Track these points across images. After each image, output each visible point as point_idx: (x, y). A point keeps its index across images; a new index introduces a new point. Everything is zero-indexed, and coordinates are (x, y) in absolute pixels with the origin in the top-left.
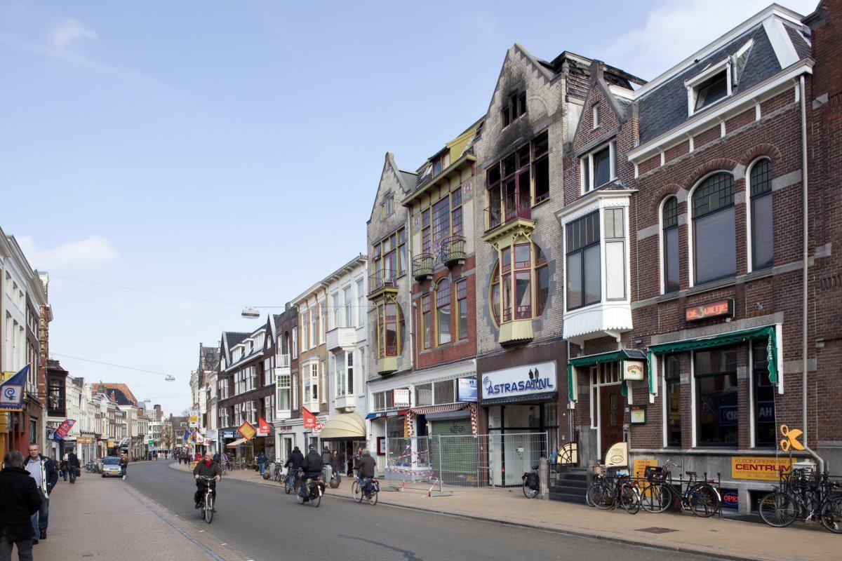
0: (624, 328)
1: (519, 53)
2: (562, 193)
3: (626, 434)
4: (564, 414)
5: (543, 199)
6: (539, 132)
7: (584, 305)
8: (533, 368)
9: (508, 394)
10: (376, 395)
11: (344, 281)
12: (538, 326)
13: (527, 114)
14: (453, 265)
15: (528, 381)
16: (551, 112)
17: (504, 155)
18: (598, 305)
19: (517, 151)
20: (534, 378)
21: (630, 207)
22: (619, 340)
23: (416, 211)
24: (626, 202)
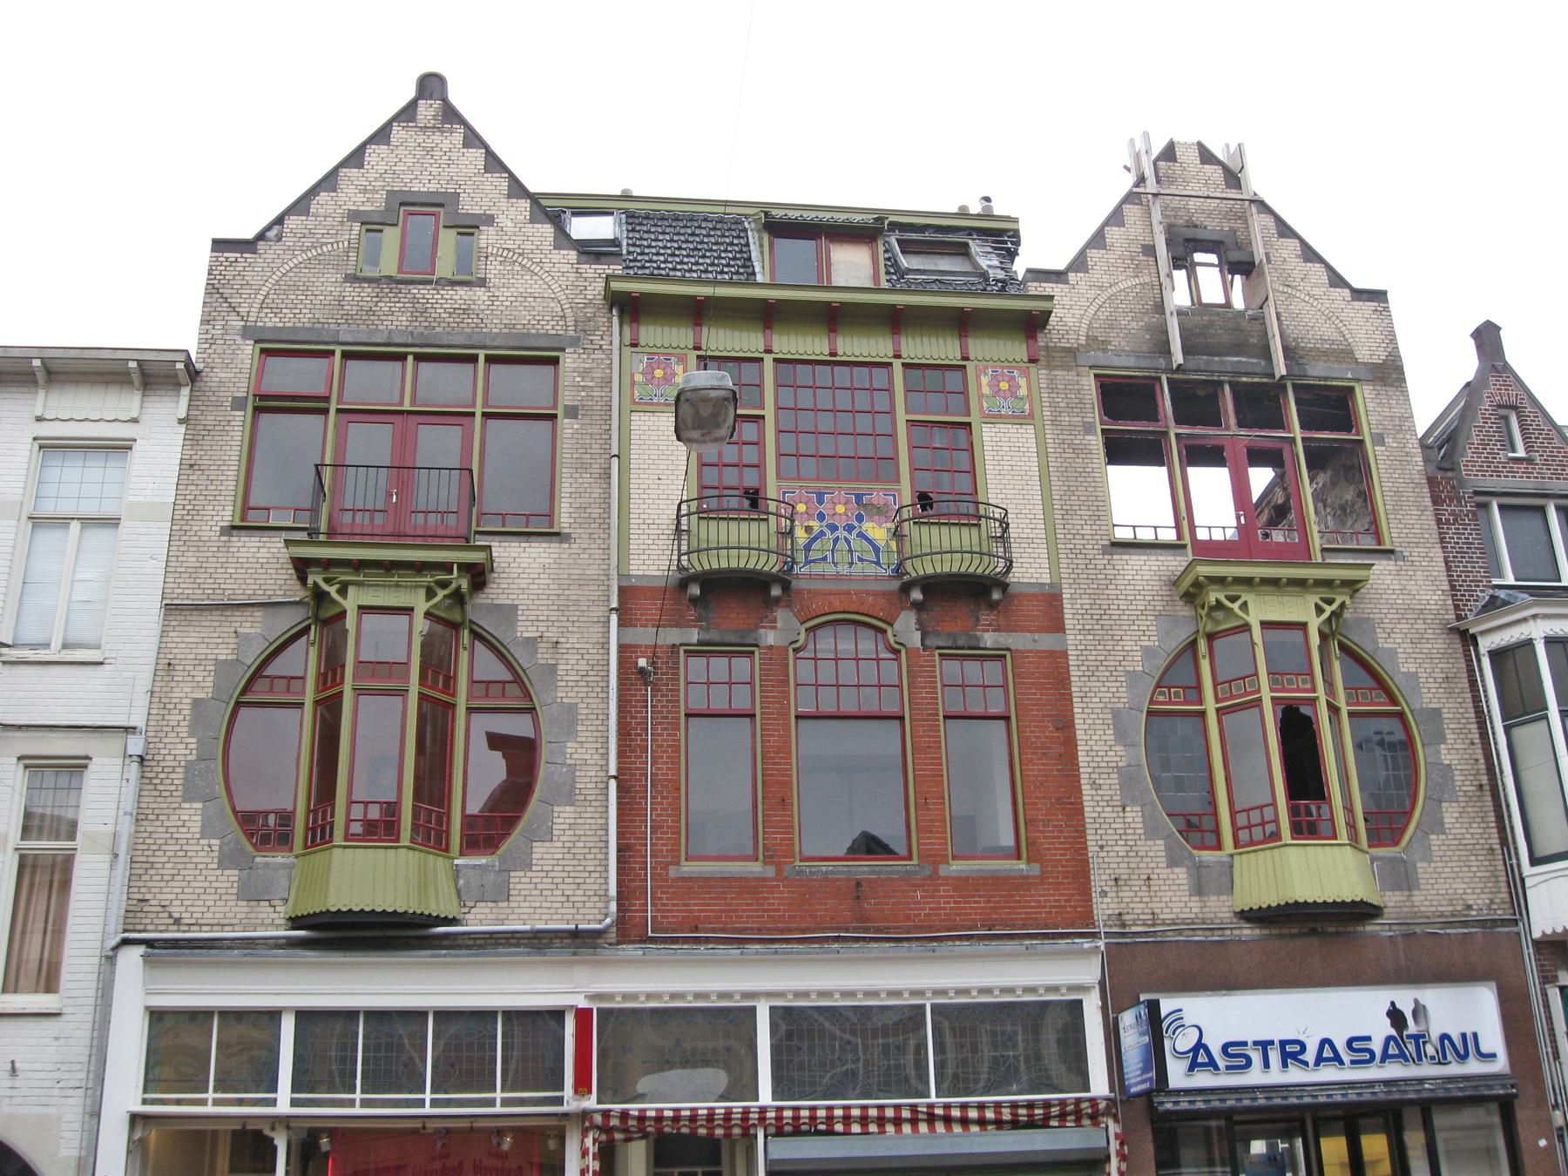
2: (1437, 554)
8: (1404, 998)
9: (1295, 1075)
15: (1389, 1039)
20: (1412, 1028)
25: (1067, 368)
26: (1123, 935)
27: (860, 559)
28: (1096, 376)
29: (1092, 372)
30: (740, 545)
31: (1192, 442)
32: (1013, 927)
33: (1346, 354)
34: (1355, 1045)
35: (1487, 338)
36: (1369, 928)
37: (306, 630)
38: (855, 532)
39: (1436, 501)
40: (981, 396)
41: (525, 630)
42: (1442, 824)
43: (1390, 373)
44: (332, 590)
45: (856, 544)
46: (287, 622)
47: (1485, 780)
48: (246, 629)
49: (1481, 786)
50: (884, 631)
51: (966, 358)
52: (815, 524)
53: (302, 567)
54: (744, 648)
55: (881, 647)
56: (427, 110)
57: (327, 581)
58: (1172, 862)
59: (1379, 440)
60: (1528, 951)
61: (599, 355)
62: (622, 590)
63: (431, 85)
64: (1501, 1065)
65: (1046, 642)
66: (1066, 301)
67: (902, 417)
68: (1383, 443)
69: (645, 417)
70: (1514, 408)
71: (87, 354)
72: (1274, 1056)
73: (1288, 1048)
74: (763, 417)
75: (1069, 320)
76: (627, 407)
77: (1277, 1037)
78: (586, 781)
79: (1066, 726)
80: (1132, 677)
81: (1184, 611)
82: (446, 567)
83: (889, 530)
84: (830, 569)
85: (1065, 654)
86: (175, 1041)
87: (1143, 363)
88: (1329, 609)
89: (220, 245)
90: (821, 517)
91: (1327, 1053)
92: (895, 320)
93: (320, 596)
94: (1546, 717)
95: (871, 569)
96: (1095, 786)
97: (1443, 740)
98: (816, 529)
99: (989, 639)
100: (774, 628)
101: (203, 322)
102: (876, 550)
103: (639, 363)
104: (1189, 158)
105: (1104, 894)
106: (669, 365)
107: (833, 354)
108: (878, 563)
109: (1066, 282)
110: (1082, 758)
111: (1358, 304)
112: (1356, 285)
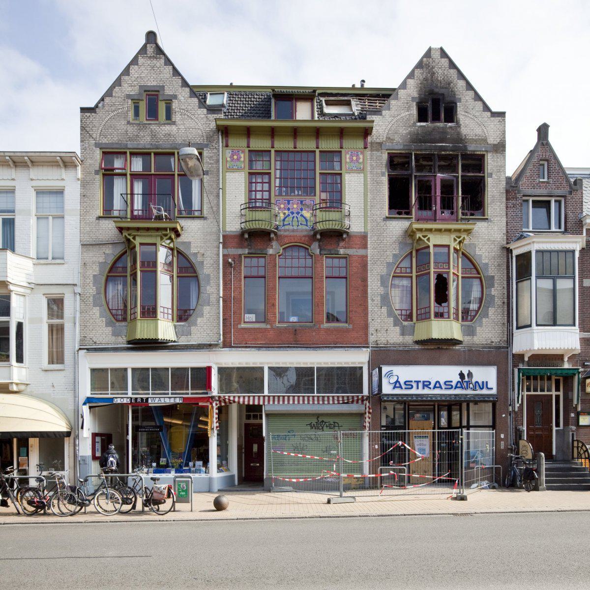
2: (504, 219)
3: (573, 434)
4: (504, 416)
6: (474, 151)
8: (465, 370)
9: (426, 391)
12: (470, 331)
20: (466, 379)
25: (377, 150)
27: (301, 224)
28: (388, 153)
29: (387, 152)
30: (262, 220)
31: (421, 179)
32: (342, 344)
33: (485, 140)
35: (543, 131)
36: (457, 348)
37: (126, 252)
38: (300, 214)
39: (507, 199)
40: (346, 162)
41: (193, 250)
42: (488, 315)
43: (500, 148)
44: (131, 238)
45: (300, 218)
46: (119, 250)
47: (506, 301)
48: (107, 252)
49: (504, 302)
50: (308, 249)
52: (286, 212)
53: (121, 229)
54: (263, 255)
55: (307, 254)
56: (150, 49)
57: (129, 235)
58: (395, 325)
59: (491, 175)
60: (510, 357)
61: (215, 151)
62: (224, 236)
63: (151, 36)
64: (494, 391)
65: (361, 252)
66: (381, 123)
67: (318, 171)
68: (491, 177)
69: (231, 174)
70: (547, 160)
71: (42, 154)
72: (420, 385)
73: (425, 383)
74: (270, 173)
75: (381, 131)
76: (225, 169)
77: (422, 380)
78: (213, 298)
79: (365, 280)
80: (388, 264)
81: (409, 241)
82: (165, 229)
83: (311, 213)
84: (291, 227)
85: (367, 256)
86: (98, 374)
87: (406, 148)
88: (458, 240)
89: (83, 110)
90: (289, 209)
91: (437, 385)
92: (318, 133)
93: (128, 240)
94: (530, 279)
95: (304, 227)
96: (373, 300)
97: (493, 286)
98: (287, 214)
99: (342, 251)
100: (272, 248)
101: (82, 141)
102: (307, 220)
103: (228, 153)
104: (436, 55)
105: (372, 334)
106: (239, 154)
107: (295, 148)
108: (307, 225)
109: (381, 115)
110: (369, 291)
111: (492, 119)
112: (494, 109)
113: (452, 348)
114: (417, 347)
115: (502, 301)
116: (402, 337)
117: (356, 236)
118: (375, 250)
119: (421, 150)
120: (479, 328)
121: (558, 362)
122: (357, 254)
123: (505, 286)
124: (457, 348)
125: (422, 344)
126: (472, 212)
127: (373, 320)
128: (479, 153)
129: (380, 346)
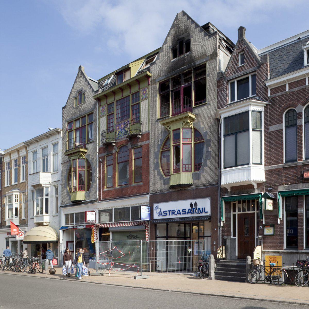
0: (259, 180)
1: (186, 16)
2: (216, 100)
4: (215, 229)
5: (201, 103)
6: (200, 64)
7: (236, 165)
8: (193, 202)
9: (174, 216)
10: (67, 216)
11: (43, 143)
12: (196, 177)
13: (192, 53)
14: (133, 138)
15: (189, 209)
16: (209, 53)
17: (173, 75)
18: (247, 166)
19: (182, 74)
20: (194, 207)
21: (264, 112)
22: (256, 187)
23: (103, 103)
24: (262, 109)
26: (153, 193)
32: (139, 194)
34: (183, 211)
36: (190, 188)
39: (218, 87)
47: (217, 153)
51: (139, 89)
58: (161, 179)
59: (209, 76)
72: (171, 213)
73: (173, 212)
77: (171, 209)
79: (148, 158)
85: (149, 144)
91: (179, 212)
96: (151, 167)
97: (209, 145)
99: (139, 144)
104: (180, 16)
107: (122, 97)
110: (150, 163)
113: (187, 189)
114: (170, 191)
115: (215, 154)
116: (164, 186)
117: (145, 134)
118: (153, 140)
119: (173, 75)
120: (202, 174)
121: (251, 189)
122: (145, 144)
123: (217, 144)
124: (190, 188)
125: (173, 189)
126: (201, 101)
127: (151, 178)
128: (203, 64)
129: (155, 192)
